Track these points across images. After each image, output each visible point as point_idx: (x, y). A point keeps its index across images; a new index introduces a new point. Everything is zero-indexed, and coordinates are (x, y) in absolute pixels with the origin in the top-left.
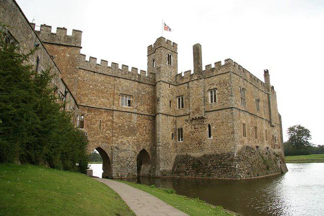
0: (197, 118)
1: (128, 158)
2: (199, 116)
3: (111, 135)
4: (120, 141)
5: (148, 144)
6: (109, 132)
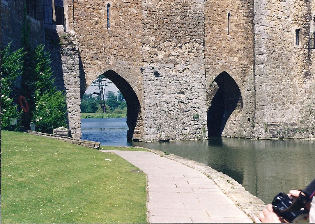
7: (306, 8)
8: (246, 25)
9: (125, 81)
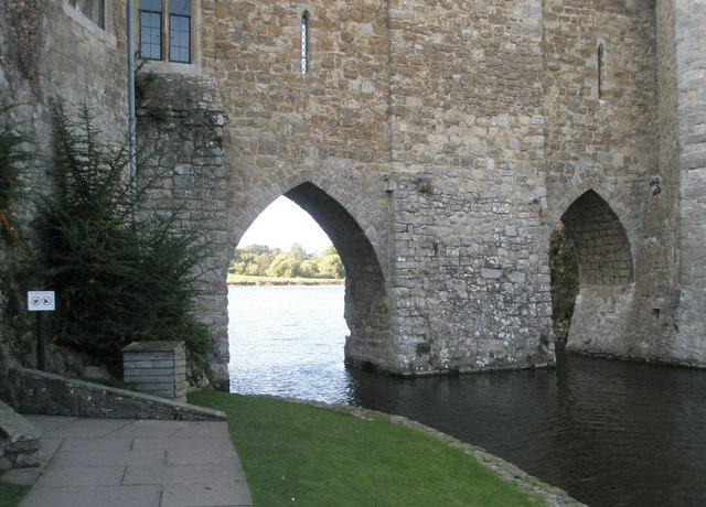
1: (493, 247)
3: (383, 107)
4: (437, 140)
5: (618, 157)
6: (368, 88)
8: (640, 77)
9: (344, 212)
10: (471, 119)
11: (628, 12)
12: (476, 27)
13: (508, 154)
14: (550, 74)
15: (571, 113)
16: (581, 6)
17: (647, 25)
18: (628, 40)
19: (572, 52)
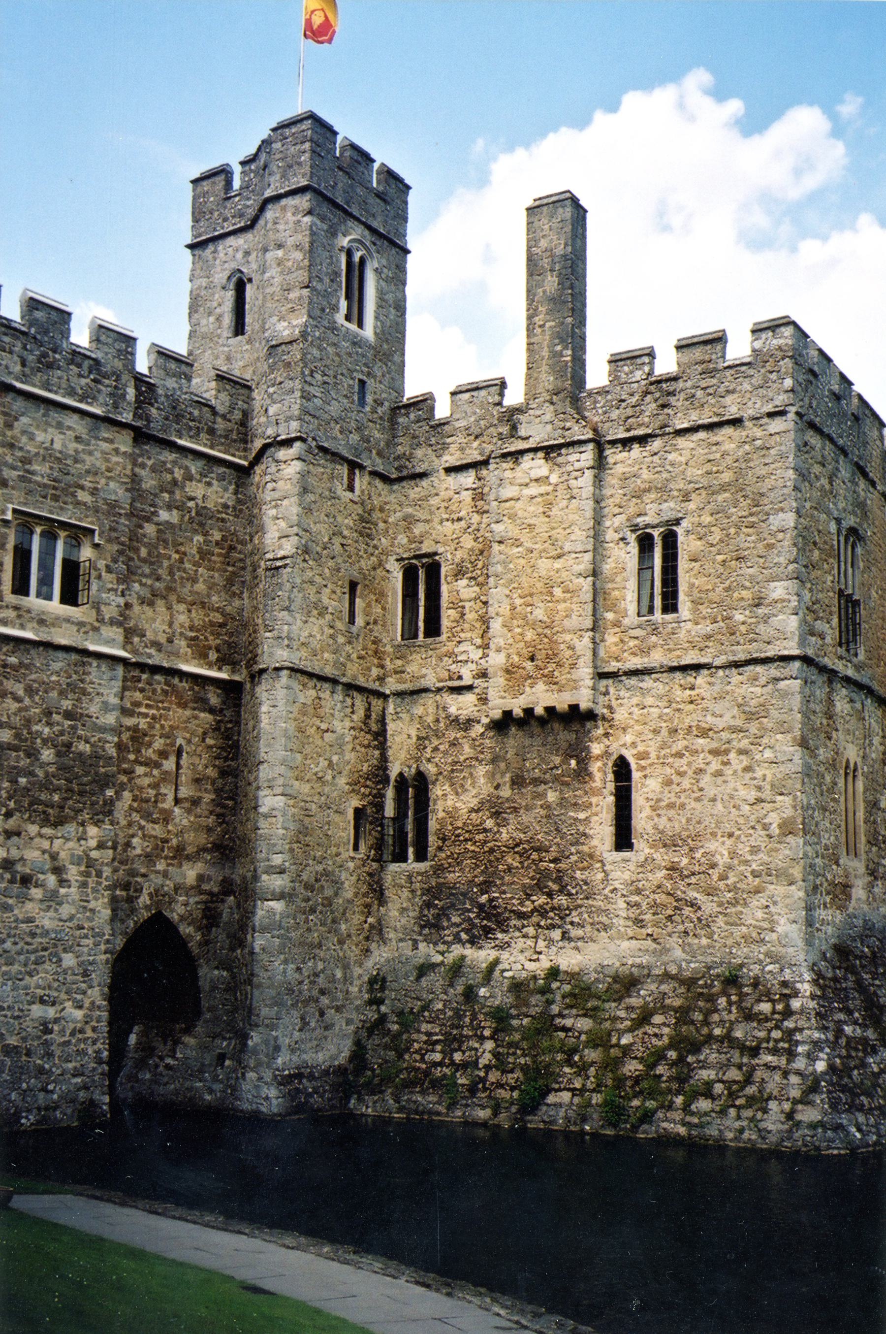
0: (539, 711)
2: (561, 701)
7: (377, 753)
10: (33, 829)
11: (211, 711)
12: (48, 724)
13: (73, 873)
14: (124, 778)
15: (143, 823)
16: (162, 702)
17: (230, 725)
18: (210, 741)
19: (150, 753)
